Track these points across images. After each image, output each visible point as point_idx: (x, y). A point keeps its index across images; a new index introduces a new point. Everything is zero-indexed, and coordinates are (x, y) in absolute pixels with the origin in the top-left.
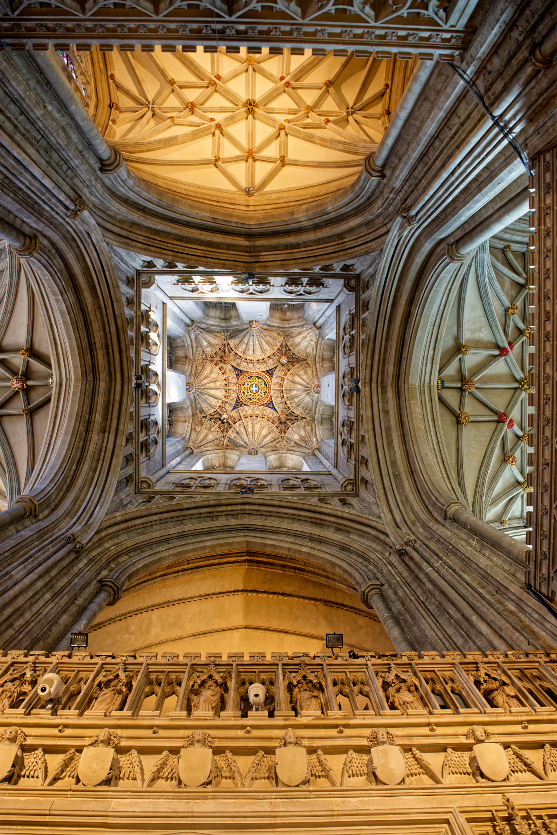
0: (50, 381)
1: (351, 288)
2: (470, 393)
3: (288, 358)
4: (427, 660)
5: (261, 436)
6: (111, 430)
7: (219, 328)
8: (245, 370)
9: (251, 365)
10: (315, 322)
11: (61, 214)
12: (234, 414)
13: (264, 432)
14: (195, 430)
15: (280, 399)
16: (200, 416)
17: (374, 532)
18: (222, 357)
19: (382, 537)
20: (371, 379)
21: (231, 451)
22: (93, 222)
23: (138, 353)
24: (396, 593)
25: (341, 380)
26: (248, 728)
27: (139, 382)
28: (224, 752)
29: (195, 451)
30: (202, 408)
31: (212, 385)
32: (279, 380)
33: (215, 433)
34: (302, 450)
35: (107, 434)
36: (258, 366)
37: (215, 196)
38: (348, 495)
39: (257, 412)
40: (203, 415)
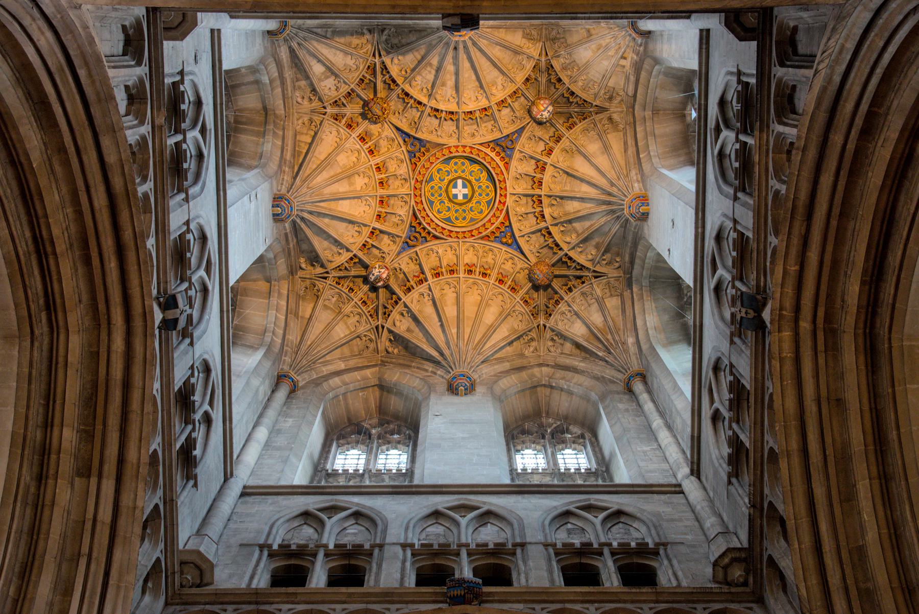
5: (482, 330)
6: (106, 468)
8: (433, 138)
9: (449, 127)
13: (490, 315)
14: (296, 315)
18: (366, 104)
29: (301, 380)
31: (342, 188)
33: (353, 320)
34: (598, 369)
36: (468, 129)
39: (469, 258)
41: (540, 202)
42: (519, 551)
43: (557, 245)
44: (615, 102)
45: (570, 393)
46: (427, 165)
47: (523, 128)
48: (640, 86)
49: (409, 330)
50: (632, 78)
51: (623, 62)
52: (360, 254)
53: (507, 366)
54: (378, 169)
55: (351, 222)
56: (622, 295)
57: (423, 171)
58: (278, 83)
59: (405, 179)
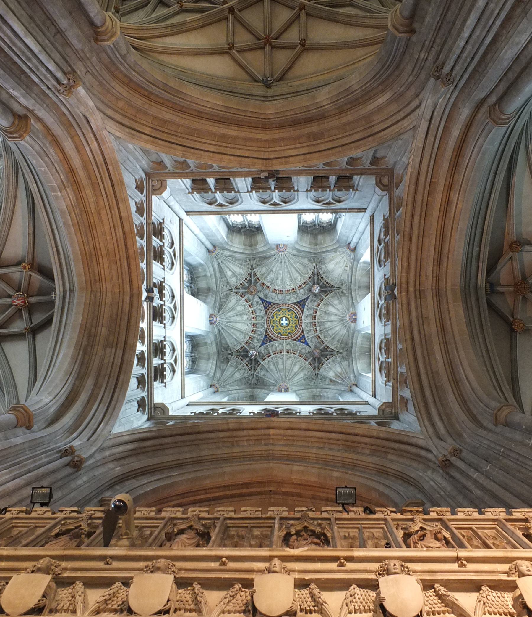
0: (53, 295)
1: (384, 186)
3: (321, 287)
4: (460, 515)
6: (119, 344)
7: (244, 256)
8: (273, 301)
9: (280, 296)
10: (349, 244)
11: (53, 89)
12: (262, 350)
13: (296, 368)
15: (312, 332)
16: (226, 353)
19: (423, 453)
21: (259, 390)
22: (91, 104)
23: (149, 266)
26: (224, 559)
28: (191, 585)
29: (220, 390)
30: (227, 344)
31: (238, 318)
32: (311, 312)
33: (242, 371)
34: (339, 387)
36: (288, 297)
38: (386, 418)
39: (288, 347)
40: (229, 352)
41: (315, 325)
43: (322, 342)
44: (344, 285)
46: (271, 311)
47: (308, 297)
48: (353, 276)
49: (264, 375)
50: (350, 275)
51: (346, 268)
52: (245, 346)
54: (252, 312)
55: (242, 332)
56: (348, 361)
57: (270, 314)
58: (213, 276)
59: (263, 317)
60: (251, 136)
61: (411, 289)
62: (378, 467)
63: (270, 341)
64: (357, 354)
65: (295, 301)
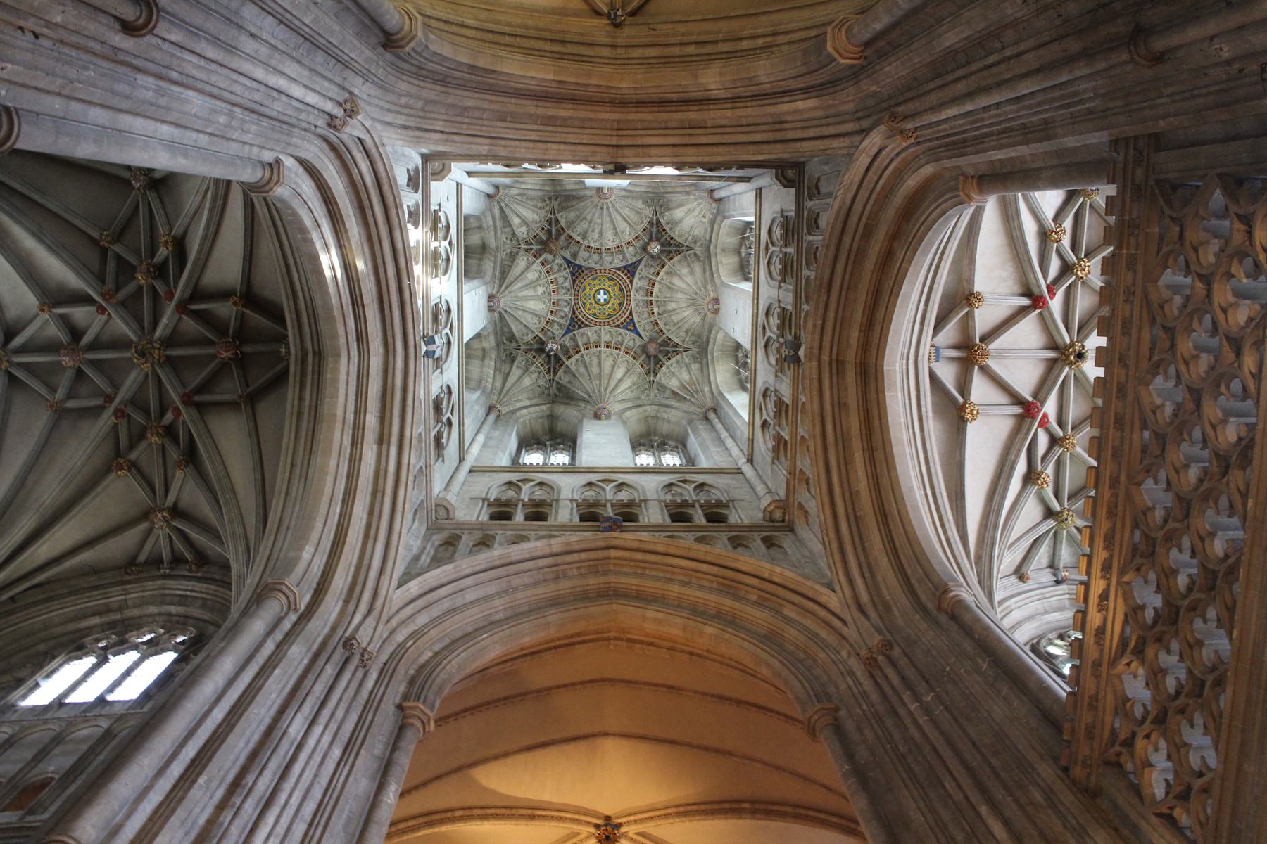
2: (982, 368)
3: (662, 245)
9: (596, 257)
12: (567, 341)
15: (646, 315)
17: (823, 613)
20: (820, 348)
24: (859, 729)
25: (762, 318)
27: (431, 348)
31: (529, 293)
32: (644, 283)
34: (686, 406)
35: (385, 446)
36: (609, 259)
37: (559, 32)
38: (777, 529)
39: (606, 338)
42: (643, 504)
44: (698, 244)
45: (669, 422)
49: (570, 382)
50: (709, 230)
51: (704, 220)
52: (540, 335)
53: (630, 404)
60: (592, 115)
61: (825, 358)
62: (770, 626)
63: (580, 327)
64: (715, 354)
65: (621, 264)
